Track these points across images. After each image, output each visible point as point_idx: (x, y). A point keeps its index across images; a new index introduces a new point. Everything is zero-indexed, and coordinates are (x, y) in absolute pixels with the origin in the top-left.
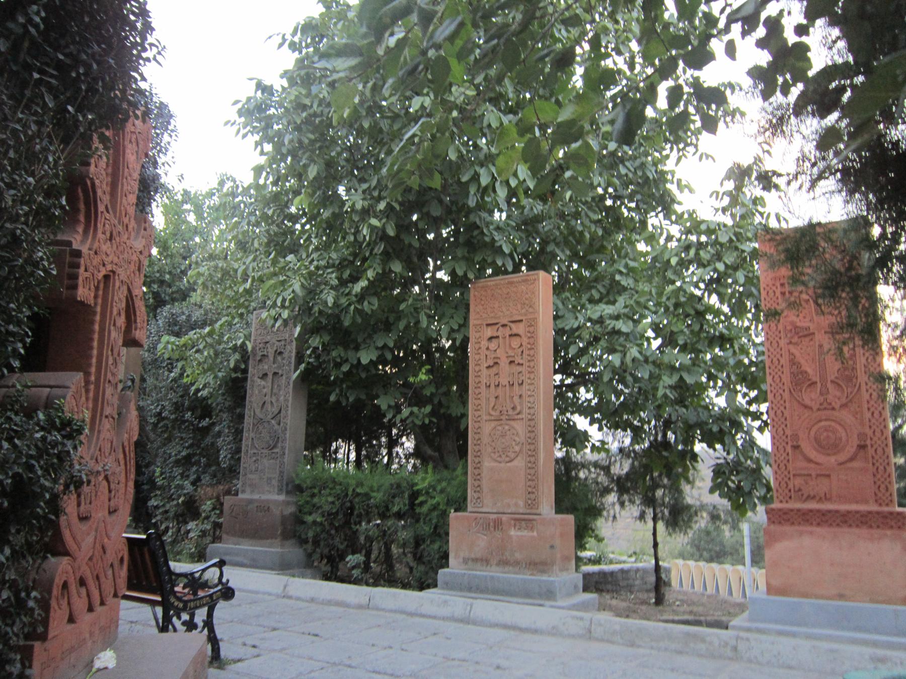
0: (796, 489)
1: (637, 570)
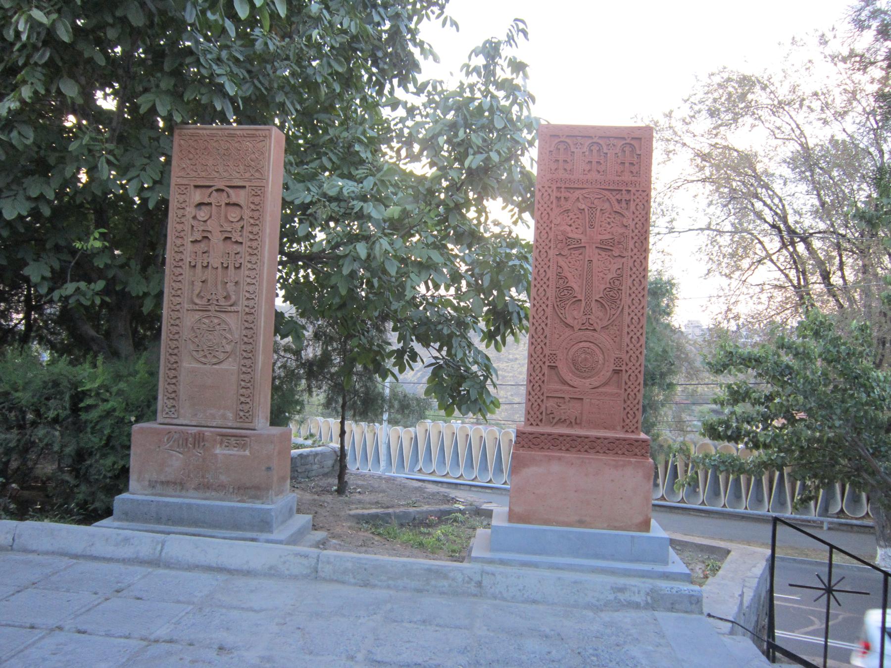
1: (316, 454)
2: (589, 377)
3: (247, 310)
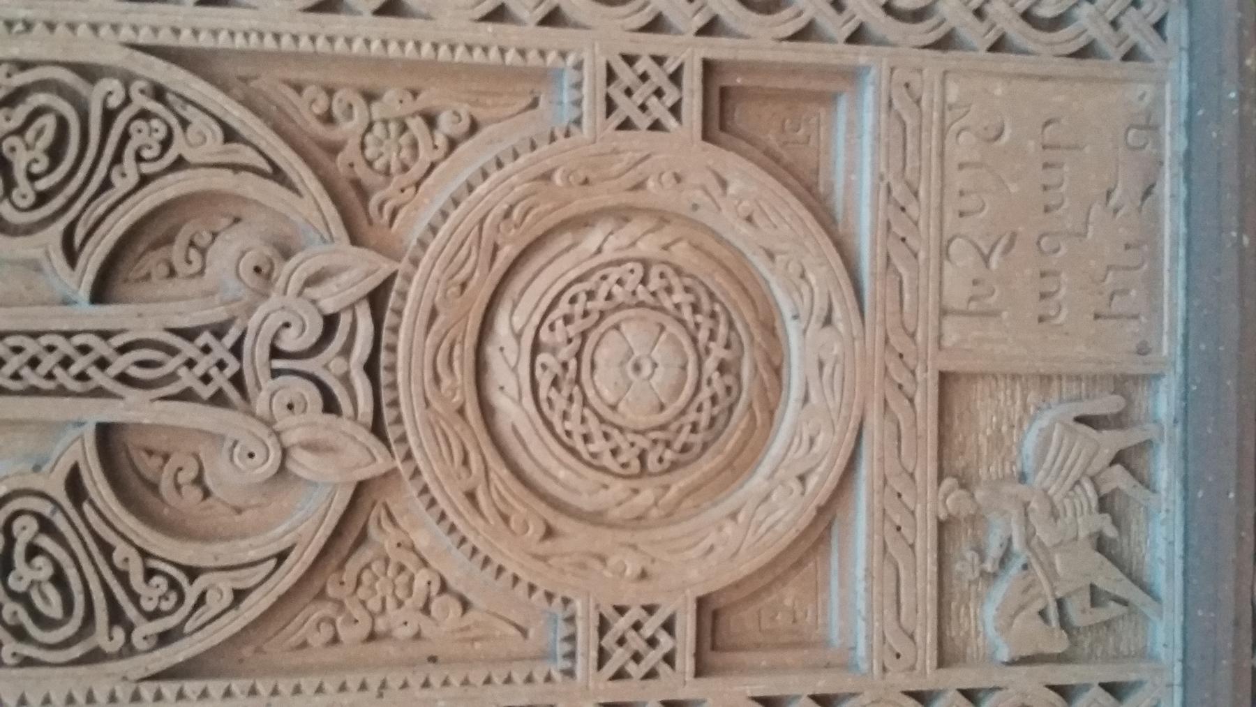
0: (1059, 643)
2: (770, 328)
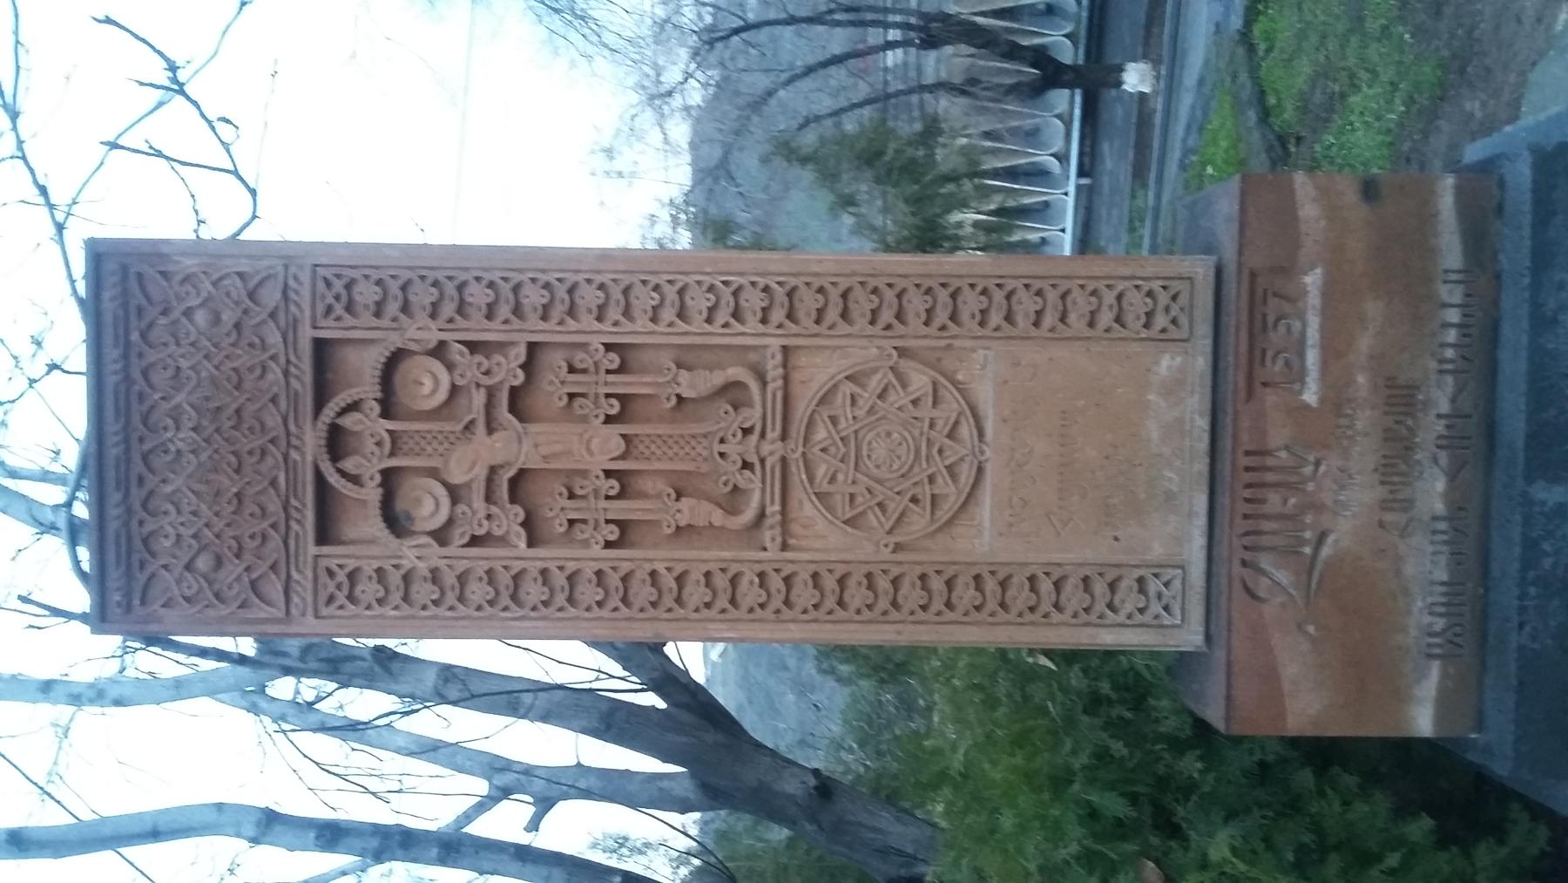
3: (778, 315)
